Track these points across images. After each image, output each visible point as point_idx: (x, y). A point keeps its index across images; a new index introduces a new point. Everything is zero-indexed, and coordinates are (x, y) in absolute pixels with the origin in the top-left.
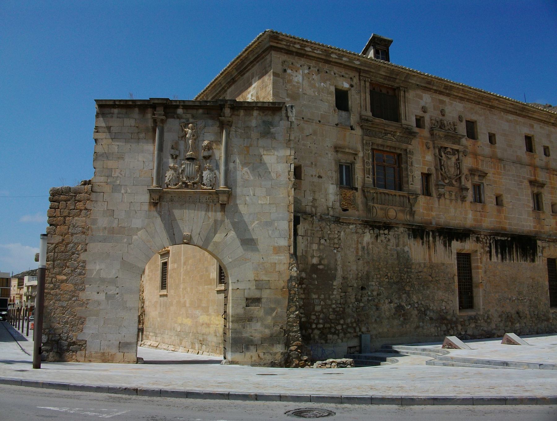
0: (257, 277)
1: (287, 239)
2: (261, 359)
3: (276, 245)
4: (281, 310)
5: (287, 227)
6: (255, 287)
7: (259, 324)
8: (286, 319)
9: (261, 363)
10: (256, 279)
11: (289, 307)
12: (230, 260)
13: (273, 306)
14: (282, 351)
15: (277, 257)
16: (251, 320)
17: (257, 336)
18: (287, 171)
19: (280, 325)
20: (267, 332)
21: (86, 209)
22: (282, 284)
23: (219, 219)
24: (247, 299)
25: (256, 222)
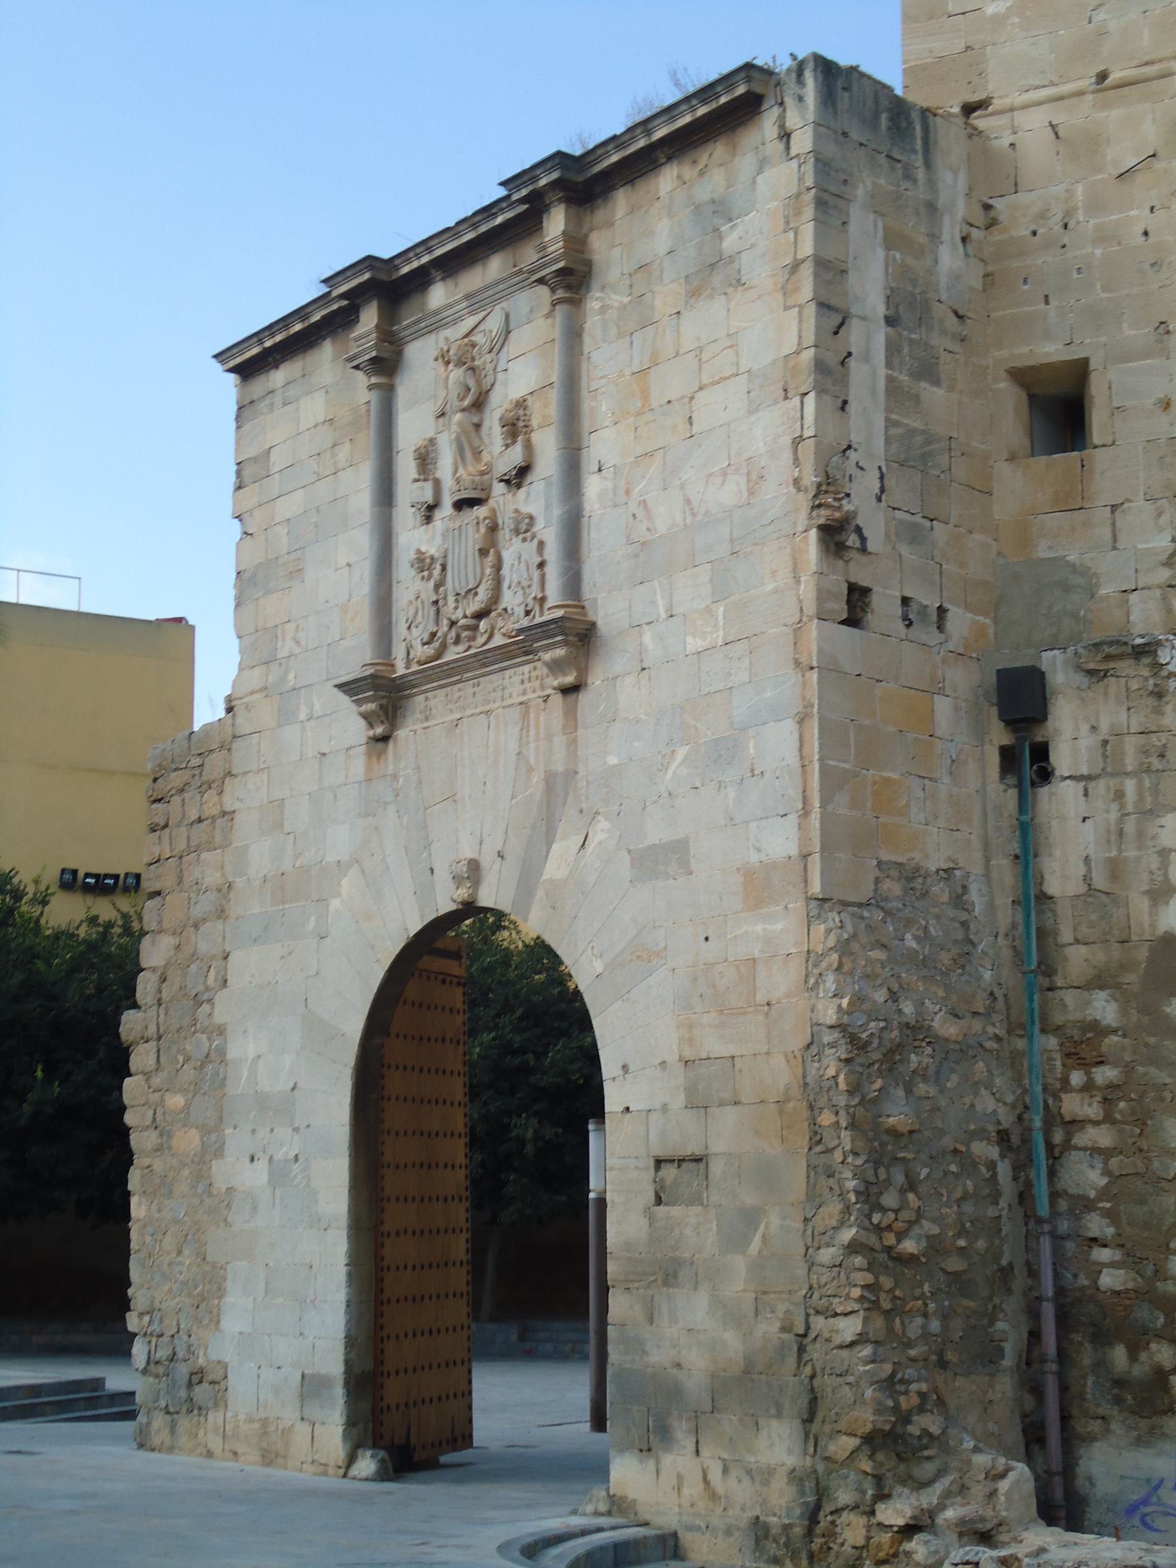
0: (691, 1040)
1: (793, 819)
2: (714, 1496)
3: (754, 858)
4: (780, 1224)
5: (793, 760)
6: (681, 1098)
7: (702, 1299)
8: (801, 1271)
9: (715, 1522)
10: (688, 1054)
11: (813, 1198)
12: (599, 966)
13: (750, 1199)
14: (791, 1461)
15: (759, 928)
16: (675, 1276)
17: (697, 1368)
18: (787, 440)
19: (781, 1308)
20: (733, 1344)
21: (224, 814)
22: (779, 1074)
23: (561, 769)
24: (659, 1163)
25: (681, 752)
